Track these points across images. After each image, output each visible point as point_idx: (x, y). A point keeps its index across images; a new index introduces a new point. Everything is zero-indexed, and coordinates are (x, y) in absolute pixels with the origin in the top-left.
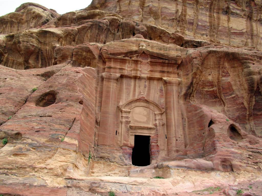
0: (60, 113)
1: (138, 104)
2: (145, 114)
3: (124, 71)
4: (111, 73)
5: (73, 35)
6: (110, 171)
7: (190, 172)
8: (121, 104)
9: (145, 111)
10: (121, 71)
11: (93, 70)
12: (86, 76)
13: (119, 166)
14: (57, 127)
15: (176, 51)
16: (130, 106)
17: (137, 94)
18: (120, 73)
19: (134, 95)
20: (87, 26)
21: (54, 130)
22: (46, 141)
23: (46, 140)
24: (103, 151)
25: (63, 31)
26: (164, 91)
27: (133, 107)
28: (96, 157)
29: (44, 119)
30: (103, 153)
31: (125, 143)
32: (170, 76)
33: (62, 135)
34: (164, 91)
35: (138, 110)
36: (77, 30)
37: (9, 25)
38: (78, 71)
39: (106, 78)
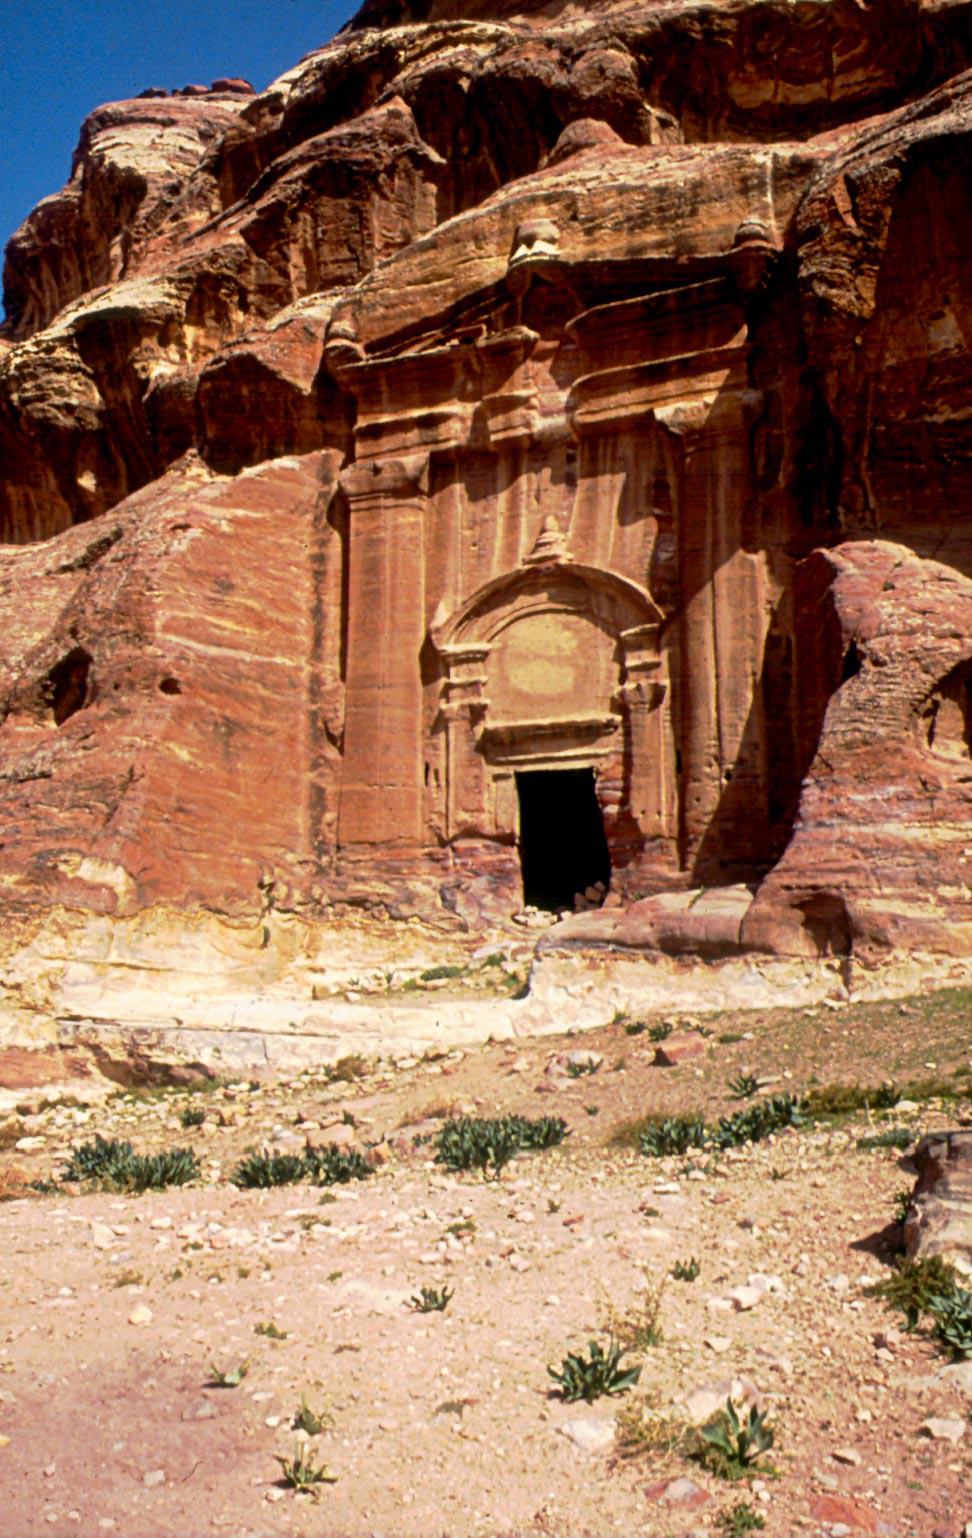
0: (80, 753)
1: (523, 601)
2: (568, 653)
3: (443, 430)
4: (380, 462)
5: (228, 279)
6: (393, 958)
7: (623, 966)
8: (443, 614)
9: (567, 634)
10: (430, 434)
11: (286, 474)
12: (225, 527)
13: (435, 934)
14: (62, 817)
15: (742, 200)
16: (485, 620)
17: (525, 541)
18: (426, 443)
19: (511, 548)
20: (281, 196)
21: (50, 833)
22: (17, 883)
23: (15, 877)
24: (363, 873)
25: (171, 280)
26: (673, 494)
27: (502, 624)
28: (325, 900)
29: (27, 789)
30: (363, 880)
31: (465, 822)
32: (700, 386)
33: (71, 851)
34: (673, 494)
35: (527, 633)
36: (242, 241)
37: (46, 274)
38: (181, 521)
39: (360, 496)
